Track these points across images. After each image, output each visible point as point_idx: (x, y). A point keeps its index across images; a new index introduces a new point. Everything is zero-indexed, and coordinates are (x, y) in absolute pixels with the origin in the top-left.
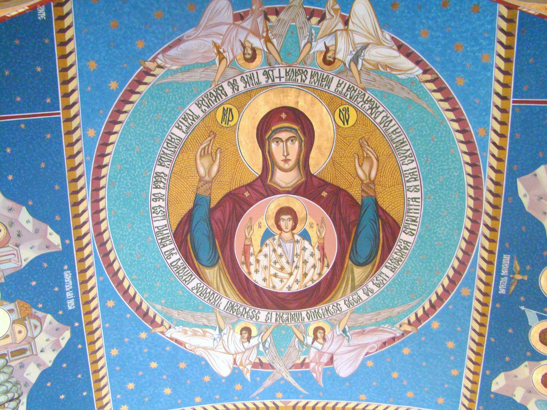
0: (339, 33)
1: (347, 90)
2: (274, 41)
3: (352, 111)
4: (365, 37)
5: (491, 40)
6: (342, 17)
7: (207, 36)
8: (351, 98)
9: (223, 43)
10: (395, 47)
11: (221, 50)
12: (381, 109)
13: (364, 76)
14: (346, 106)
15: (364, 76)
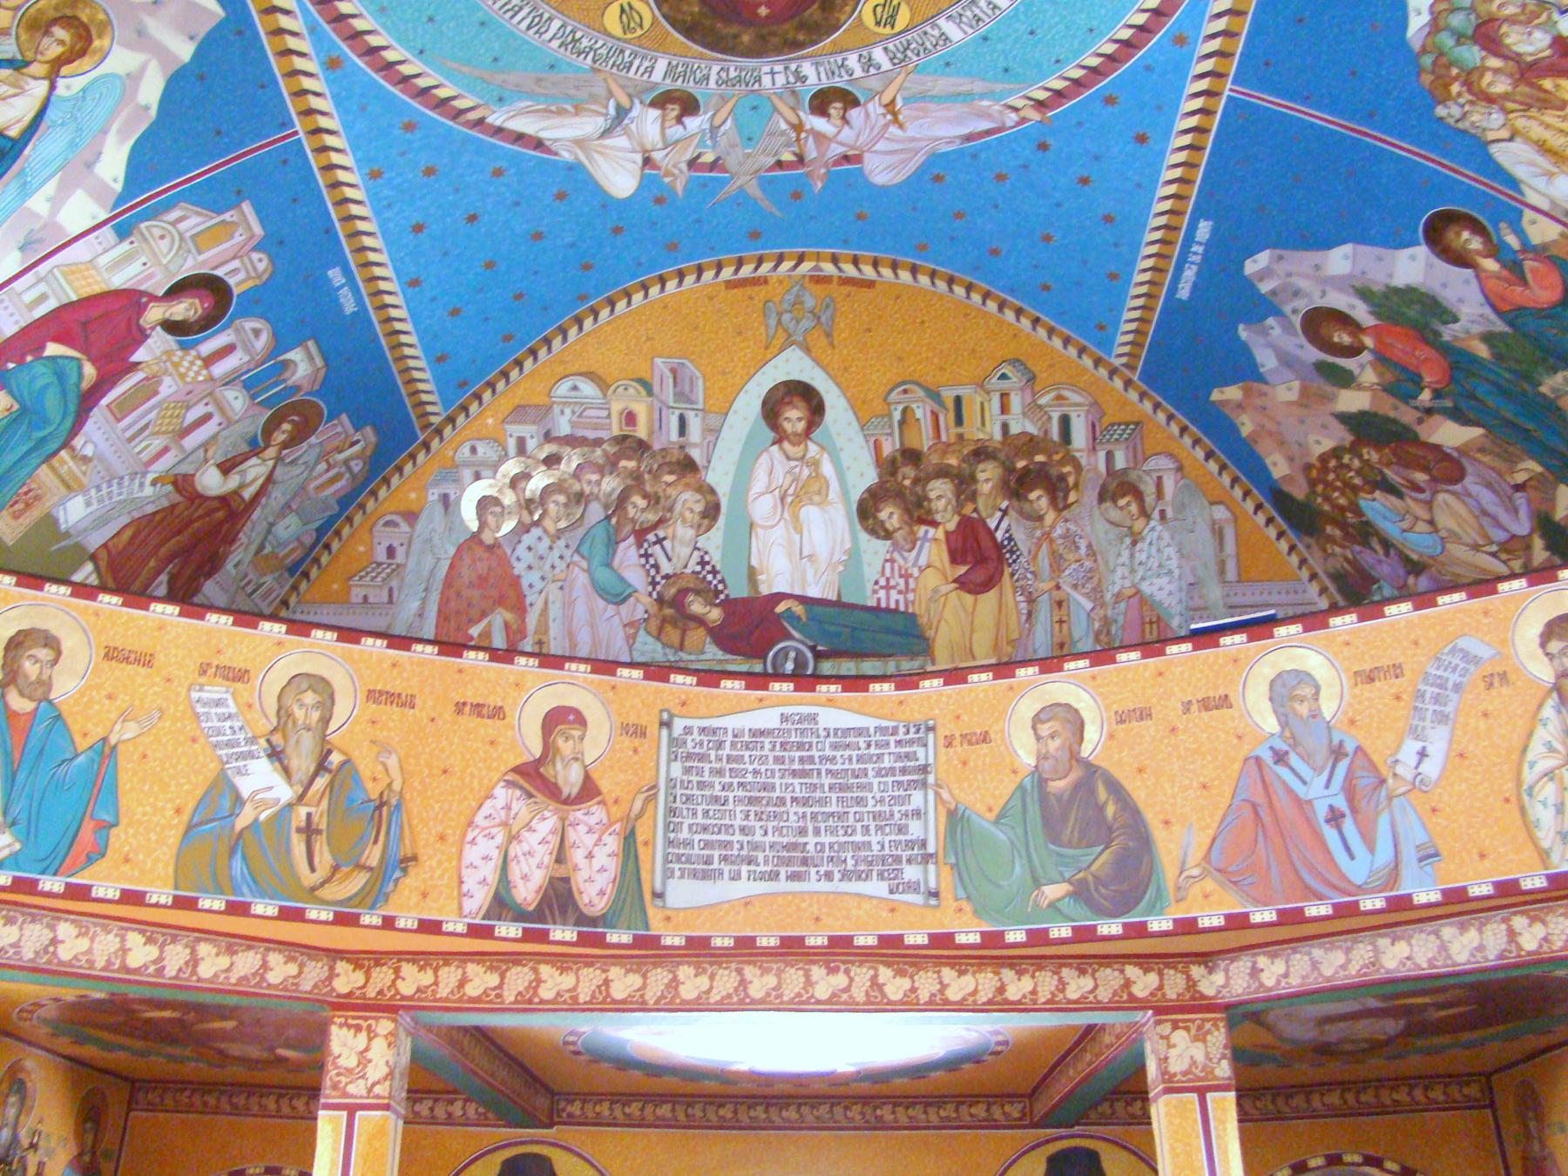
0: (660, 145)
1: (631, 64)
2: (784, 126)
3: (617, 30)
4: (605, 147)
5: (374, 197)
6: (655, 167)
7: (913, 139)
8: (622, 52)
9: (886, 126)
10: (548, 143)
11: (889, 117)
12: (555, 44)
13: (600, 91)
14: (629, 36)
15: (600, 91)
